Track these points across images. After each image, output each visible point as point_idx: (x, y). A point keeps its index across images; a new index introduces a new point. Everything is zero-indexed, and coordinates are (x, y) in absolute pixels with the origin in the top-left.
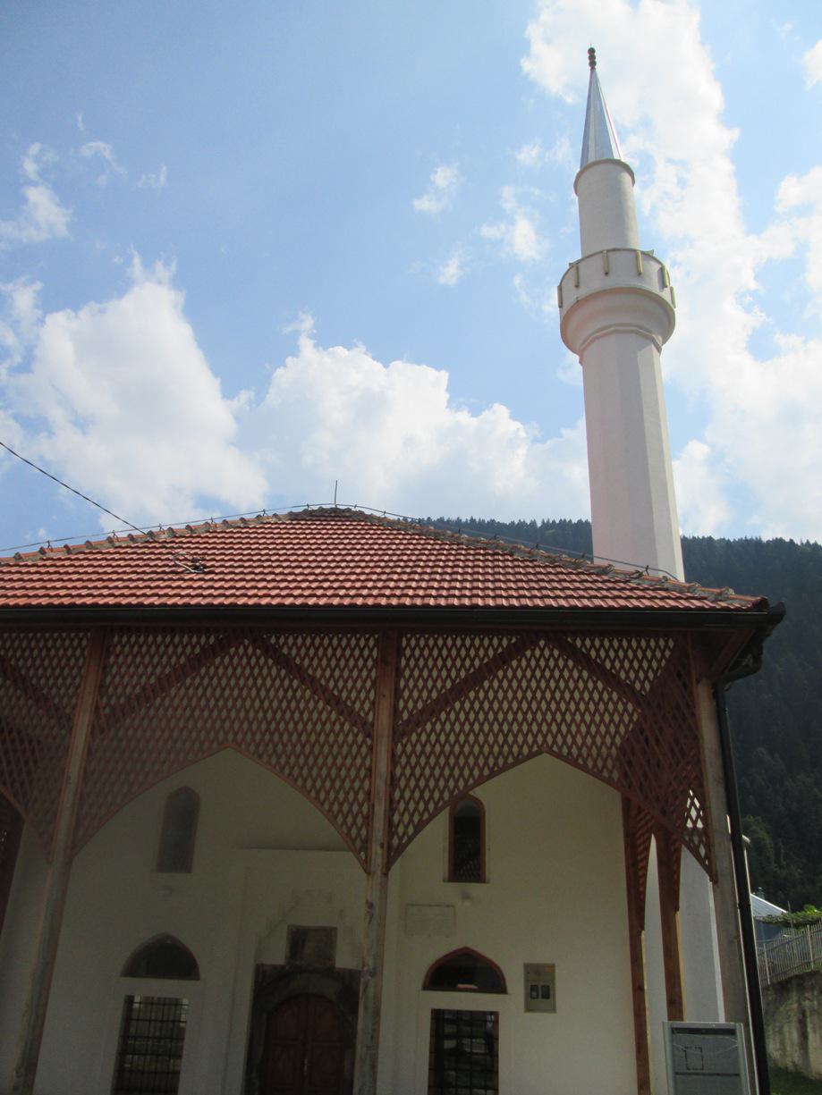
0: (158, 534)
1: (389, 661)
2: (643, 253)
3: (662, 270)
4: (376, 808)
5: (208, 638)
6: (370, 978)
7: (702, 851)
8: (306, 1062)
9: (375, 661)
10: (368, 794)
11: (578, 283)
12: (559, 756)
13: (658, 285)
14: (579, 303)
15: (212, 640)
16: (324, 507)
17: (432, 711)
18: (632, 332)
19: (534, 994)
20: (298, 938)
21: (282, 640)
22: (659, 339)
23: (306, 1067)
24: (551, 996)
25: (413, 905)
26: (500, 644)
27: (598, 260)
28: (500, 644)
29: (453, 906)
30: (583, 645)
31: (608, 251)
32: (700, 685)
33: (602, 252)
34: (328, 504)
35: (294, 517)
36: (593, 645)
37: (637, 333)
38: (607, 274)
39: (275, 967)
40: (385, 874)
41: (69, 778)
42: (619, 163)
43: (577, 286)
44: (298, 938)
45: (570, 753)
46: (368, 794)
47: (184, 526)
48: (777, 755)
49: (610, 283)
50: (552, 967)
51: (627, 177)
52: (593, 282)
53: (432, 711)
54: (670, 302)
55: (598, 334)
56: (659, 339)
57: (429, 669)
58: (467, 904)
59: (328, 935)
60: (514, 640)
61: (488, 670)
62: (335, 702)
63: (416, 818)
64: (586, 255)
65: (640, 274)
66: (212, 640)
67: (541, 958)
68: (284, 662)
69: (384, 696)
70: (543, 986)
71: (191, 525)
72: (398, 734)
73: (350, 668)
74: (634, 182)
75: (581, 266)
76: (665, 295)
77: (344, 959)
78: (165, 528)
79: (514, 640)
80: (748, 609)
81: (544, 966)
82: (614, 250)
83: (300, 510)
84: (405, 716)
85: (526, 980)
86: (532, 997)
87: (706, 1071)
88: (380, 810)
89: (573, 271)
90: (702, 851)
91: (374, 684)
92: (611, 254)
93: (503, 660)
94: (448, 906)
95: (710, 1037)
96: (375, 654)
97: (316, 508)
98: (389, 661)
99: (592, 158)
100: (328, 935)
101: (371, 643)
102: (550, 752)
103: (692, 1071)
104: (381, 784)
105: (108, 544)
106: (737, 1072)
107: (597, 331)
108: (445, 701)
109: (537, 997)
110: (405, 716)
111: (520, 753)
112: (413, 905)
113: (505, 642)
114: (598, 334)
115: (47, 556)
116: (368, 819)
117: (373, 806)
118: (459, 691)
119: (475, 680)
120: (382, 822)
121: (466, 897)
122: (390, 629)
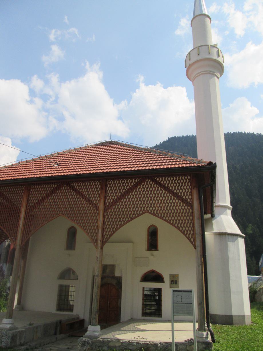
0: (54, 154)
1: (104, 188)
2: (211, 46)
3: (218, 50)
4: (99, 230)
5: (55, 185)
6: (96, 277)
7: (192, 240)
8: (108, 302)
9: (100, 189)
10: (97, 227)
12: (151, 213)
13: (216, 56)
14: (190, 66)
15: (56, 186)
16: (107, 141)
17: (115, 202)
18: (208, 73)
19: (173, 283)
20: (105, 268)
21: (74, 184)
22: (218, 75)
23: (108, 304)
24: (177, 284)
25: (137, 258)
26: (135, 181)
27: (196, 49)
28: (135, 181)
29: (148, 258)
30: (159, 180)
31: (199, 47)
32: (194, 190)
33: (197, 47)
34: (108, 140)
35: (97, 145)
36: (162, 180)
38: (198, 55)
40: (102, 248)
41: (20, 226)
42: (205, 15)
43: (190, 60)
44: (105, 268)
45: (154, 212)
46: (97, 227)
47: (62, 151)
49: (200, 58)
50: (178, 275)
51: (208, 19)
52: (194, 58)
53: (115, 202)
54: (222, 62)
56: (218, 75)
57: (115, 189)
58: (152, 257)
59: (113, 267)
60: (139, 180)
61: (131, 189)
62: (88, 201)
63: (110, 233)
64: (194, 48)
65: (210, 53)
66: (56, 186)
67: (174, 272)
68: (75, 190)
69: (102, 199)
70: (175, 281)
71: (64, 151)
72: (106, 210)
73: (93, 191)
74: (211, 21)
76: (220, 59)
77: (117, 274)
78: (56, 152)
79: (139, 180)
80: (206, 166)
81: (175, 275)
82: (201, 46)
83: (100, 143)
84: (108, 204)
85: (170, 279)
86: (172, 284)
87: (182, 302)
88: (100, 231)
90: (192, 240)
91: (99, 196)
92: (200, 48)
93: (135, 186)
94: (147, 258)
95: (184, 293)
96: (100, 186)
97: (105, 142)
98: (104, 188)
99: (195, 15)
100: (113, 267)
101: (99, 183)
102: (148, 212)
103: (178, 302)
104: (101, 224)
105: (39, 159)
106: (191, 303)
107: (196, 75)
108: (119, 199)
109: (173, 284)
110: (108, 204)
111: (140, 213)
112: (137, 258)
113: (136, 181)
114: (197, 75)
115: (21, 164)
116: (97, 233)
117: (98, 230)
118: (123, 196)
119: (127, 193)
120: (101, 234)
121: (152, 255)
122: (104, 179)
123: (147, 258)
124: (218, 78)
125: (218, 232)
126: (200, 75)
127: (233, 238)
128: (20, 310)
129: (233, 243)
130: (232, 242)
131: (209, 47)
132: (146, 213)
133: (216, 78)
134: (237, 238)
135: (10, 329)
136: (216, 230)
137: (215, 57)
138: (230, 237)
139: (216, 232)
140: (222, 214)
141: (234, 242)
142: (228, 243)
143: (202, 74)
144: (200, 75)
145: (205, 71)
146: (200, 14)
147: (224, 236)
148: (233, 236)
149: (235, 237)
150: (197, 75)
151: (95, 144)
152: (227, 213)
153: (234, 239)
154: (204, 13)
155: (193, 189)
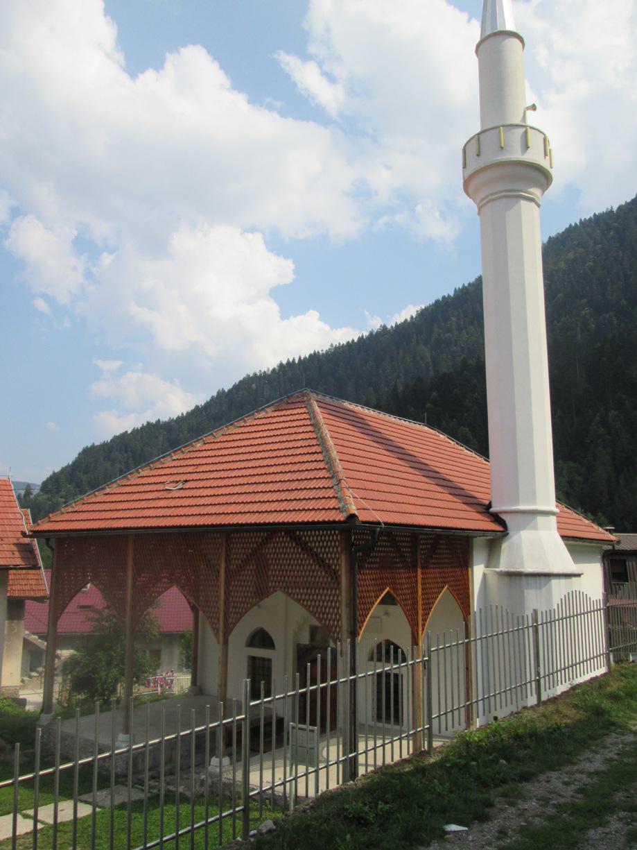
11: (479, 152)
13: (520, 149)
31: (479, 134)
37: (506, 197)
38: (478, 155)
39: (304, 645)
48: (600, 514)
49: (482, 162)
51: (516, 42)
52: (473, 165)
55: (490, 198)
56: (535, 192)
65: (502, 148)
72: (227, 582)
75: (482, 137)
76: (534, 155)
89: (474, 141)
94: (378, 617)
116: (218, 619)
121: (387, 614)
123: (378, 617)
124: (531, 200)
125: (506, 570)
126: (487, 203)
128: (195, 695)
129: (538, 591)
130: (536, 588)
131: (500, 132)
133: (523, 203)
134: (549, 580)
136: (503, 566)
137: (517, 155)
138: (530, 580)
139: (501, 572)
140: (524, 529)
141: (540, 588)
142: (526, 592)
143: (490, 201)
144: (487, 203)
145: (496, 193)
146: (491, 32)
147: (518, 578)
148: (538, 578)
149: (543, 579)
150: (484, 202)
152: (536, 524)
154: (500, 28)
155: (342, 553)
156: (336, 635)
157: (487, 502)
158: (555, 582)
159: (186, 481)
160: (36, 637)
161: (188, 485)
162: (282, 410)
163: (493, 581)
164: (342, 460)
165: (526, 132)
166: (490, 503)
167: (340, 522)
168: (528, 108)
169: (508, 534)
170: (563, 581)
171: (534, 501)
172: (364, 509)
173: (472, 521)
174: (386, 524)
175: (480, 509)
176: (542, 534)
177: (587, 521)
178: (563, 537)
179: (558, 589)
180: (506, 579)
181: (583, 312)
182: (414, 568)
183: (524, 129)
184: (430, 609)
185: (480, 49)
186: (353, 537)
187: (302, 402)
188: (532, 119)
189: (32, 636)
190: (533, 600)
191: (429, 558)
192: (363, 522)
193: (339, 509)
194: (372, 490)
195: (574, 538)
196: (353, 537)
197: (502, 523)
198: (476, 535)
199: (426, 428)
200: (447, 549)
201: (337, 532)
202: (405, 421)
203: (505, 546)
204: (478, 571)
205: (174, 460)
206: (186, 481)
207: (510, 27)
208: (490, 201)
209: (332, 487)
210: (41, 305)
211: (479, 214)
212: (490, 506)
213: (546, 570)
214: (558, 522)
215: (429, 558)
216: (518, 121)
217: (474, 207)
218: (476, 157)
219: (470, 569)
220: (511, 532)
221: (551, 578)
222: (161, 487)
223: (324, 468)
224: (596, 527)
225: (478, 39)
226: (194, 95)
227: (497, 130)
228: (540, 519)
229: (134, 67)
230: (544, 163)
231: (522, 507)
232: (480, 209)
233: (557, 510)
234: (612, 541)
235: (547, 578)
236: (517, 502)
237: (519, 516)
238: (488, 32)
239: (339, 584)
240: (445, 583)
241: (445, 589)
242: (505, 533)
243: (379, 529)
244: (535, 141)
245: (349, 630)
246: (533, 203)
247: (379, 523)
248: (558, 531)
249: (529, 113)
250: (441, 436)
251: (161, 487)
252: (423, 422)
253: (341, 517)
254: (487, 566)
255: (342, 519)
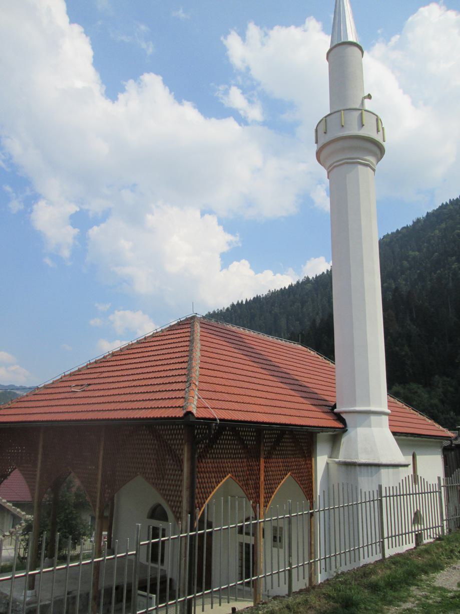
0: (107, 356)
31: (326, 117)
38: (325, 133)
51: (356, 49)
52: (323, 140)
55: (335, 164)
56: (371, 159)
64: (332, 112)
65: (343, 126)
76: (369, 131)
97: (184, 319)
125: (344, 460)
127: (370, 471)
131: (341, 114)
132: (138, 475)
133: (360, 167)
134: (379, 470)
135: (29, 603)
136: (341, 458)
138: (364, 469)
140: (360, 426)
141: (372, 476)
142: (359, 479)
143: (335, 167)
146: (336, 43)
147: (353, 467)
148: (369, 467)
149: (374, 468)
151: (168, 326)
153: (372, 472)
156: (178, 515)
157: (333, 403)
158: (383, 471)
159: (89, 385)
160: (11, 504)
161: (90, 388)
162: (174, 330)
163: (334, 468)
164: (202, 368)
165: (362, 114)
166: (335, 405)
167: (179, 418)
168: (365, 98)
169: (347, 430)
170: (391, 470)
171: (368, 402)
172: (205, 408)
173: (313, 418)
174: (220, 420)
175: (327, 409)
176: (375, 430)
177: (430, 421)
178: (394, 433)
179: (388, 479)
180: (343, 468)
181: (453, 267)
182: (258, 458)
183: (360, 112)
184: (273, 493)
185: (330, 54)
186: (196, 431)
187: (189, 323)
188: (368, 105)
189: (8, 504)
190: (366, 484)
191: (280, 450)
192: (198, 418)
193: (182, 407)
194: (221, 392)
195: (407, 434)
196: (196, 431)
197: (343, 421)
198: (317, 431)
199: (300, 346)
200: (290, 442)
201: (182, 426)
202: (282, 340)
203: (344, 439)
204: (321, 461)
205: (89, 368)
206: (89, 385)
207: (352, 38)
208: (335, 167)
209: (184, 390)
210: (47, 261)
211: (328, 178)
212: (335, 407)
213: (376, 461)
214: (389, 420)
215: (280, 450)
216: (358, 106)
217: (324, 172)
218: (324, 134)
219: (313, 459)
220: (349, 429)
221: (381, 468)
222: (68, 389)
223: (185, 374)
224: (437, 425)
225: (328, 48)
226: (155, 113)
227: (339, 113)
228: (373, 418)
229: (113, 91)
230: (378, 138)
231: (357, 408)
232: (328, 173)
233: (389, 411)
234: (450, 437)
235: (377, 468)
236: (355, 405)
237: (356, 414)
238: (336, 43)
239: (182, 471)
240: (289, 471)
241: (287, 476)
242: (344, 430)
243: (214, 424)
244: (369, 121)
245: (188, 510)
246: (369, 168)
247: (215, 419)
248: (390, 428)
249: (367, 101)
250: (312, 352)
251: (68, 389)
252: (298, 341)
253: (180, 413)
254: (330, 457)
255: (181, 416)
